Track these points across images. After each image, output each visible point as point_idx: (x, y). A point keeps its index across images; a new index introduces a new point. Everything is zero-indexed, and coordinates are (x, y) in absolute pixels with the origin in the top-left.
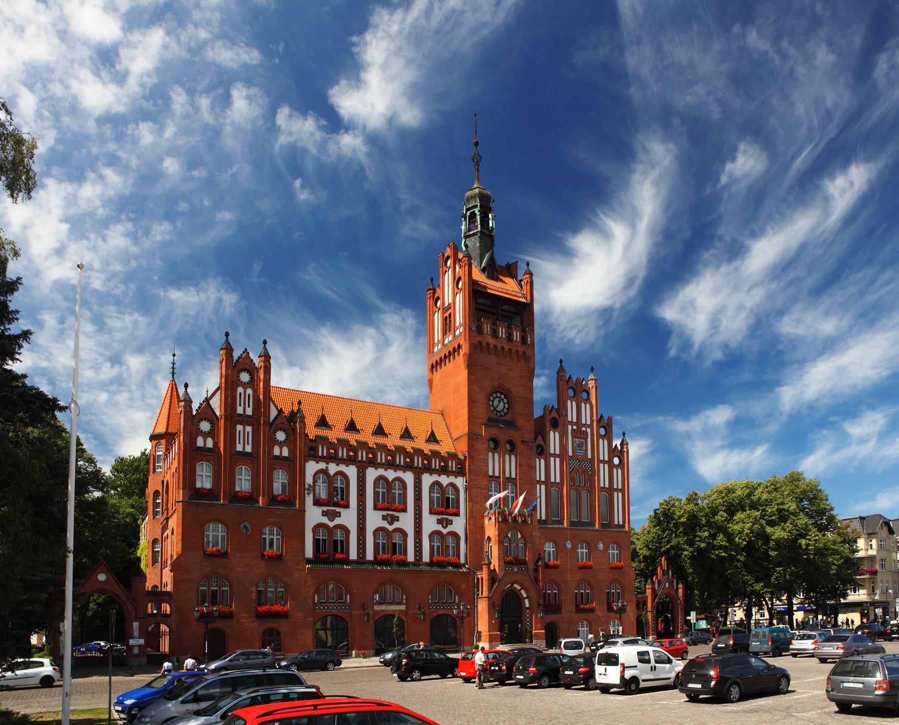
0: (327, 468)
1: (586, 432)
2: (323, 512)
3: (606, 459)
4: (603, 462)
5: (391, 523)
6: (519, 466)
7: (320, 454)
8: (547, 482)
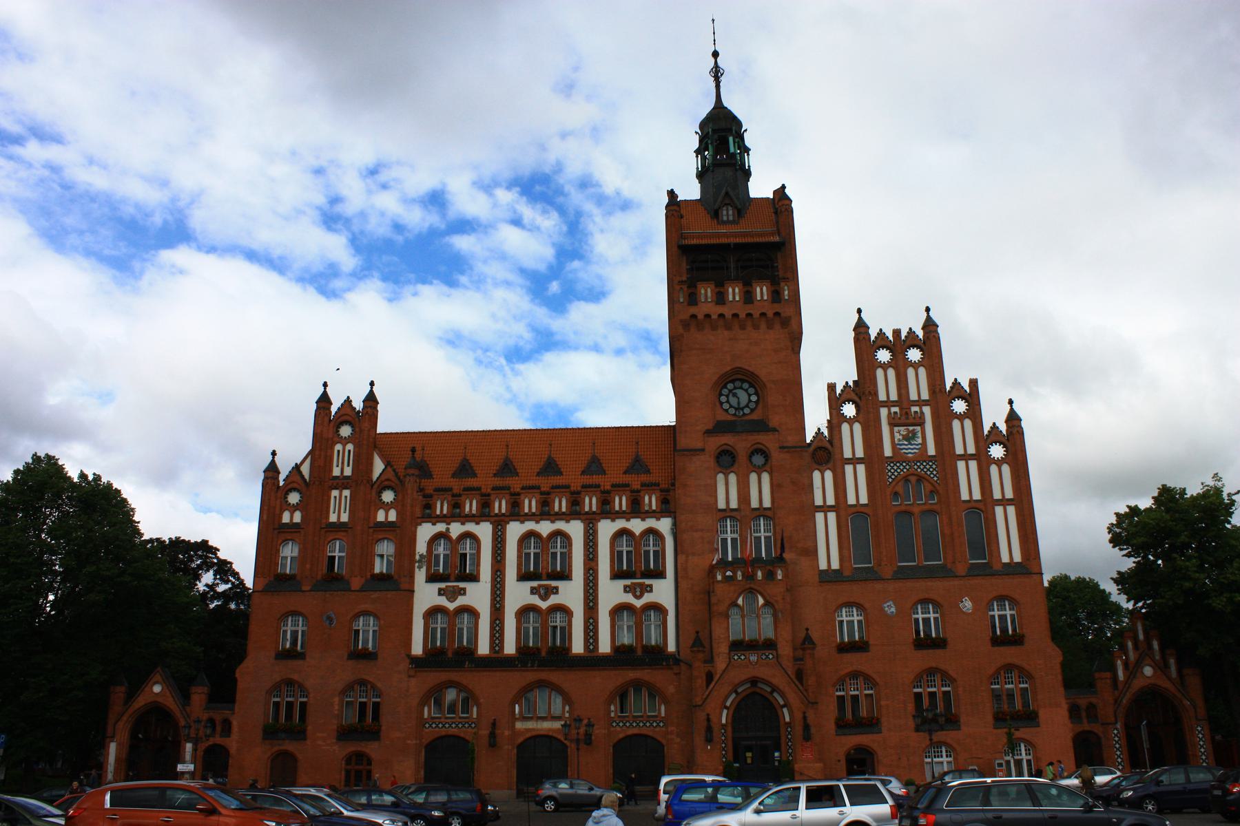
0: (448, 529)
1: (922, 413)
2: (440, 590)
3: (971, 450)
4: (966, 457)
5: (544, 598)
7: (438, 512)
8: (840, 506)
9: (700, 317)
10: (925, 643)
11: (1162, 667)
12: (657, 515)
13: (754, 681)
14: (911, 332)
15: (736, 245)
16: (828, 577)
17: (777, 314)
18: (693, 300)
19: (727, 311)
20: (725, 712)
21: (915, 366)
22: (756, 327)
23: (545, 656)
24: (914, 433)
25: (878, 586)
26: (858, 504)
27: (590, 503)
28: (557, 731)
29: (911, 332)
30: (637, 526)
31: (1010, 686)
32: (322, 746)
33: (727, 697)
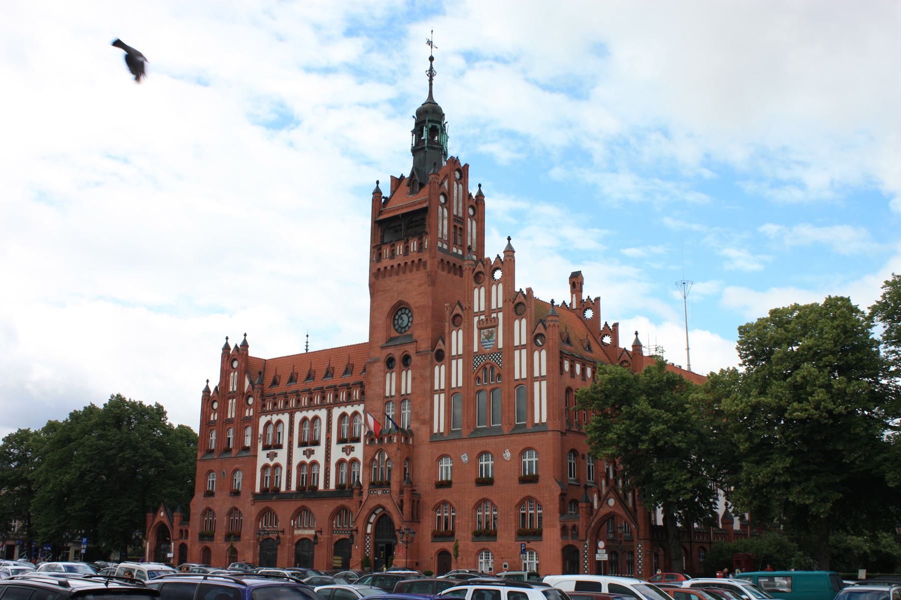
6: (413, 379)
9: (382, 269)
11: (621, 500)
12: (359, 402)
13: (384, 509)
15: (403, 215)
16: (435, 438)
17: (420, 260)
19: (395, 263)
20: (370, 526)
22: (411, 271)
23: (307, 490)
24: (492, 333)
25: (460, 443)
26: (457, 387)
27: (330, 398)
28: (311, 535)
30: (349, 410)
31: (532, 512)
32: (220, 545)
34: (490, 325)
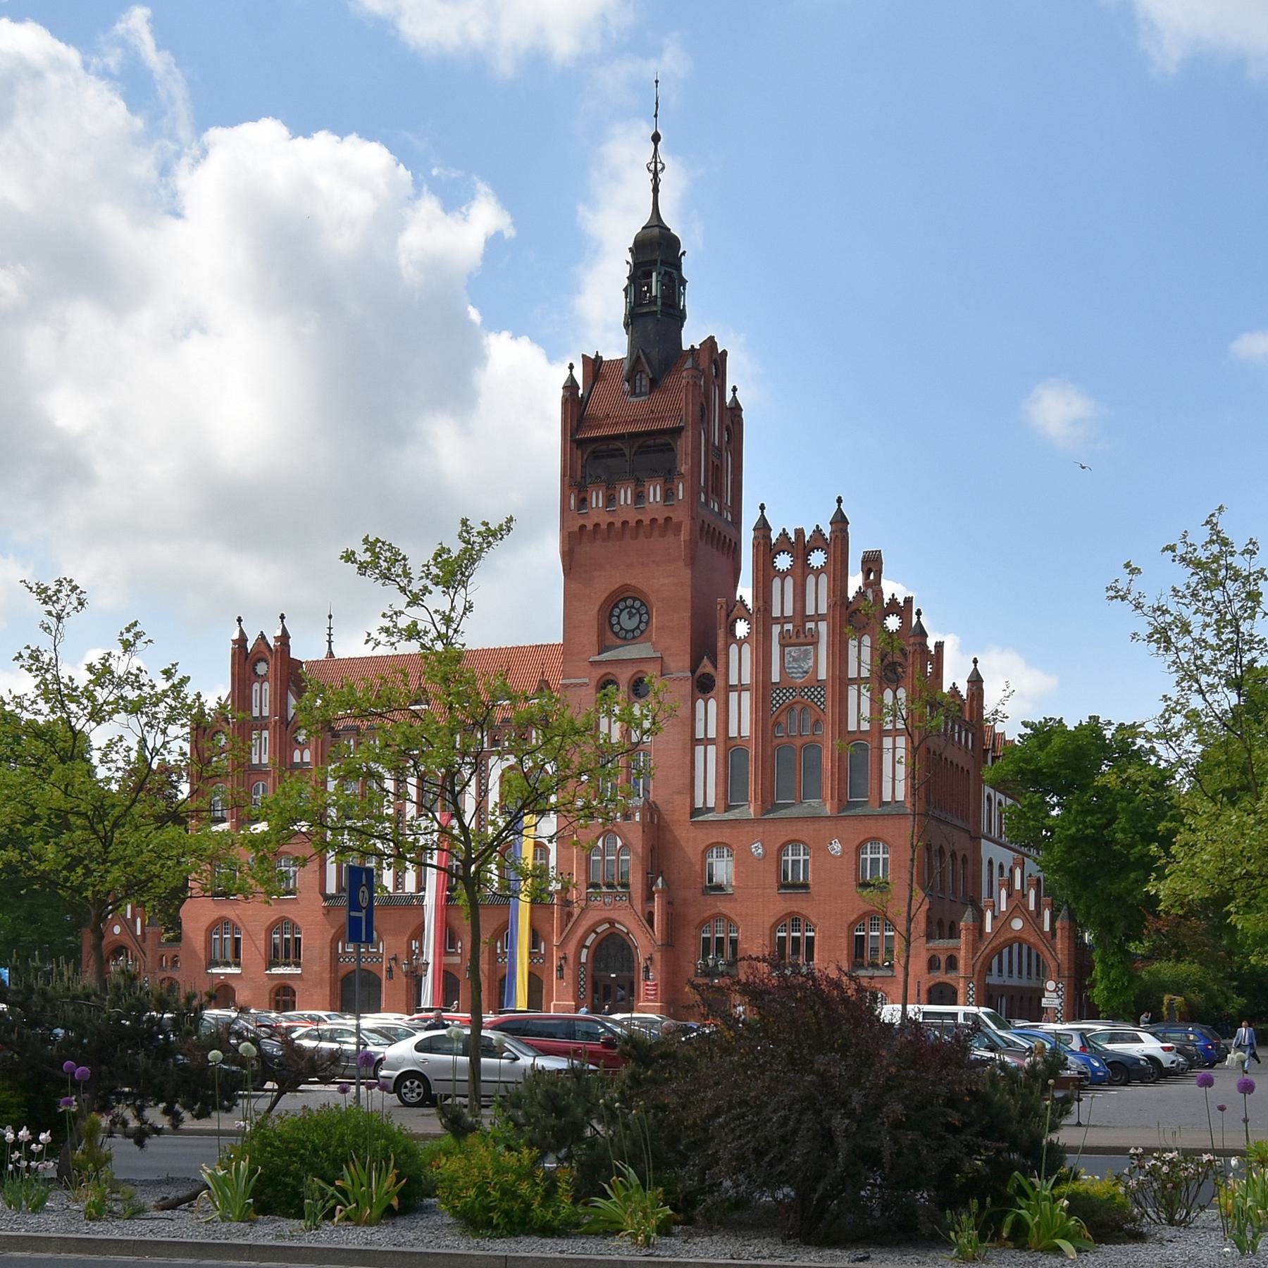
10: (788, 886)
13: (612, 923)
14: (818, 531)
15: (633, 436)
18: (582, 502)
20: (585, 951)
21: (818, 572)
24: (806, 654)
29: (818, 531)
33: (585, 937)
34: (802, 639)
